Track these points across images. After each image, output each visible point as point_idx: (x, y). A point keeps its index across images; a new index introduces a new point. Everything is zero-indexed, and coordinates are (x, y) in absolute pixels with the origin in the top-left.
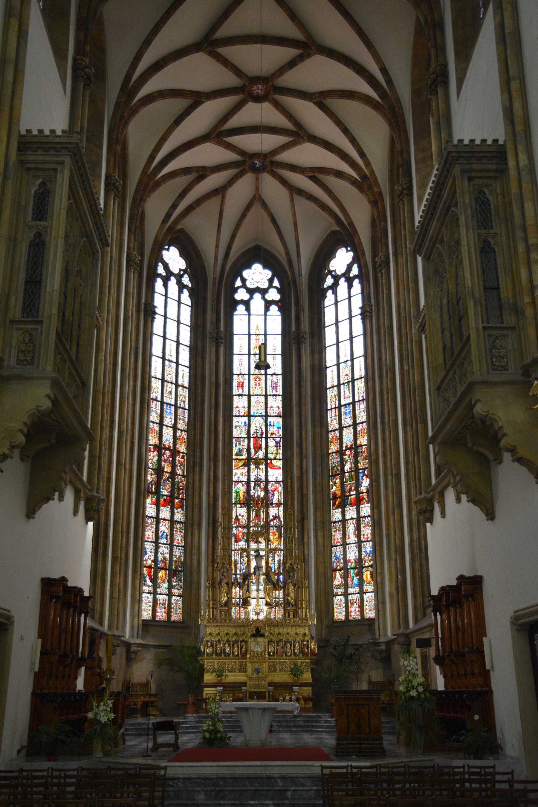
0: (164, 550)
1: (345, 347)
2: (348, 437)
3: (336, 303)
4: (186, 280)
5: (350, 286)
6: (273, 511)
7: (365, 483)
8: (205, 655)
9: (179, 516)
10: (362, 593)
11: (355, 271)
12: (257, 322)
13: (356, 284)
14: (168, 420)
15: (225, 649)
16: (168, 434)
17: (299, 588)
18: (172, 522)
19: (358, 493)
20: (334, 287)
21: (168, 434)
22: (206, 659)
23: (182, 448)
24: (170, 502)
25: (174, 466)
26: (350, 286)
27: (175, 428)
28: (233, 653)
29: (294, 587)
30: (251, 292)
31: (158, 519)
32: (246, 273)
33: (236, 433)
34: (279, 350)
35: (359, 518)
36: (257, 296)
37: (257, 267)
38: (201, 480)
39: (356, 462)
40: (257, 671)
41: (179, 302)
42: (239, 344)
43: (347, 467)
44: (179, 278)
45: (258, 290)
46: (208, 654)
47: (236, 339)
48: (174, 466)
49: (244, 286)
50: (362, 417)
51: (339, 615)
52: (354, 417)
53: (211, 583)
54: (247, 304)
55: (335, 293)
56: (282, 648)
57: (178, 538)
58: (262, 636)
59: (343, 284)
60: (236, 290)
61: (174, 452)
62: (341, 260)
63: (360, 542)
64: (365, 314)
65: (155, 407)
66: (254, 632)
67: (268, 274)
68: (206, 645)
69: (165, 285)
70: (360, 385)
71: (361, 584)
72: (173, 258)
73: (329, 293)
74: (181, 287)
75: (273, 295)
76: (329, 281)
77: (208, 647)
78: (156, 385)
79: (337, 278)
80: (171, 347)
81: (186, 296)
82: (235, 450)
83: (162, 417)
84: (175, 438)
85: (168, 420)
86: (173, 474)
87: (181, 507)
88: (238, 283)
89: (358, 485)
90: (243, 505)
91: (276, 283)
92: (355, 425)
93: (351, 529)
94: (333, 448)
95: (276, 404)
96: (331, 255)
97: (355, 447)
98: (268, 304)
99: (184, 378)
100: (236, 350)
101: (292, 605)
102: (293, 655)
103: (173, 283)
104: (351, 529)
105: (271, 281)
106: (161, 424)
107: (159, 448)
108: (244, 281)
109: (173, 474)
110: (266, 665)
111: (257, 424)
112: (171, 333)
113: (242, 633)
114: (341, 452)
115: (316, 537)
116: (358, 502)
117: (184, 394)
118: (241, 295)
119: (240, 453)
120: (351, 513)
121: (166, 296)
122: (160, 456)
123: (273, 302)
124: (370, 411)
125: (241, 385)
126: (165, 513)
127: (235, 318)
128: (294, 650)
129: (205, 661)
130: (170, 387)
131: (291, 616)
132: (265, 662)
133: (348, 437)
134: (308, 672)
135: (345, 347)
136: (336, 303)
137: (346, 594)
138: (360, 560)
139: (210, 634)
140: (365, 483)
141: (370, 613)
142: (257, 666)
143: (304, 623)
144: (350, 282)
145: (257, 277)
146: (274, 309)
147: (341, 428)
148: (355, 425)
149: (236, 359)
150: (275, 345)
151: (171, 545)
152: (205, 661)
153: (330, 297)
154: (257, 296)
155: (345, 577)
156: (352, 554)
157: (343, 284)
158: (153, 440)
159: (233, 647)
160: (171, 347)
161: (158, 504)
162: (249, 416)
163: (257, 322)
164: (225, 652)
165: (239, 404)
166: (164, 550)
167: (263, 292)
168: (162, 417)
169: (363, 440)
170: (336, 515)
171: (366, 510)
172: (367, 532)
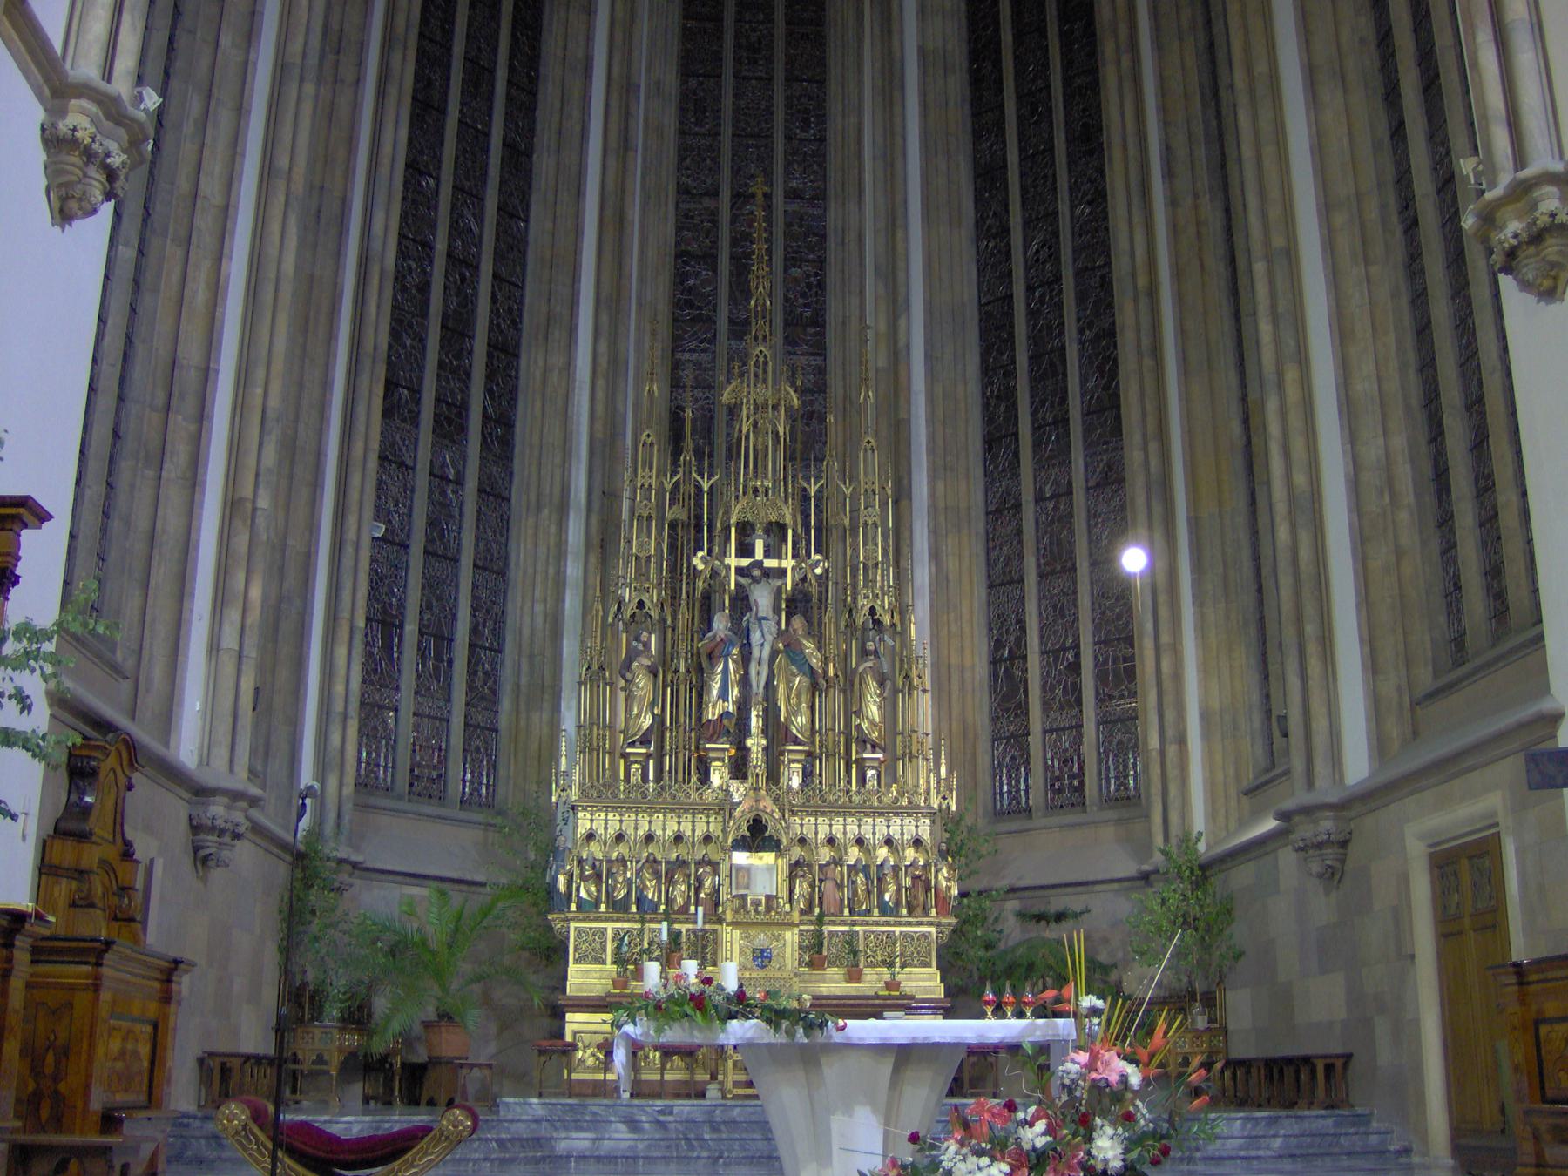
8: (573, 907)
15: (642, 889)
17: (895, 691)
22: (574, 919)
28: (669, 902)
29: (881, 684)
38: (569, 367)
40: (762, 957)
46: (581, 904)
53: (595, 667)
56: (840, 886)
58: (774, 845)
66: (744, 831)
68: (576, 871)
77: (583, 878)
101: (873, 747)
102: (876, 912)
110: (791, 937)
113: (699, 833)
115: (936, 556)
128: (881, 895)
129: (573, 925)
131: (872, 784)
132: (791, 925)
134: (926, 965)
139: (590, 836)
142: (761, 939)
152: (573, 925)
159: (670, 880)
164: (640, 901)
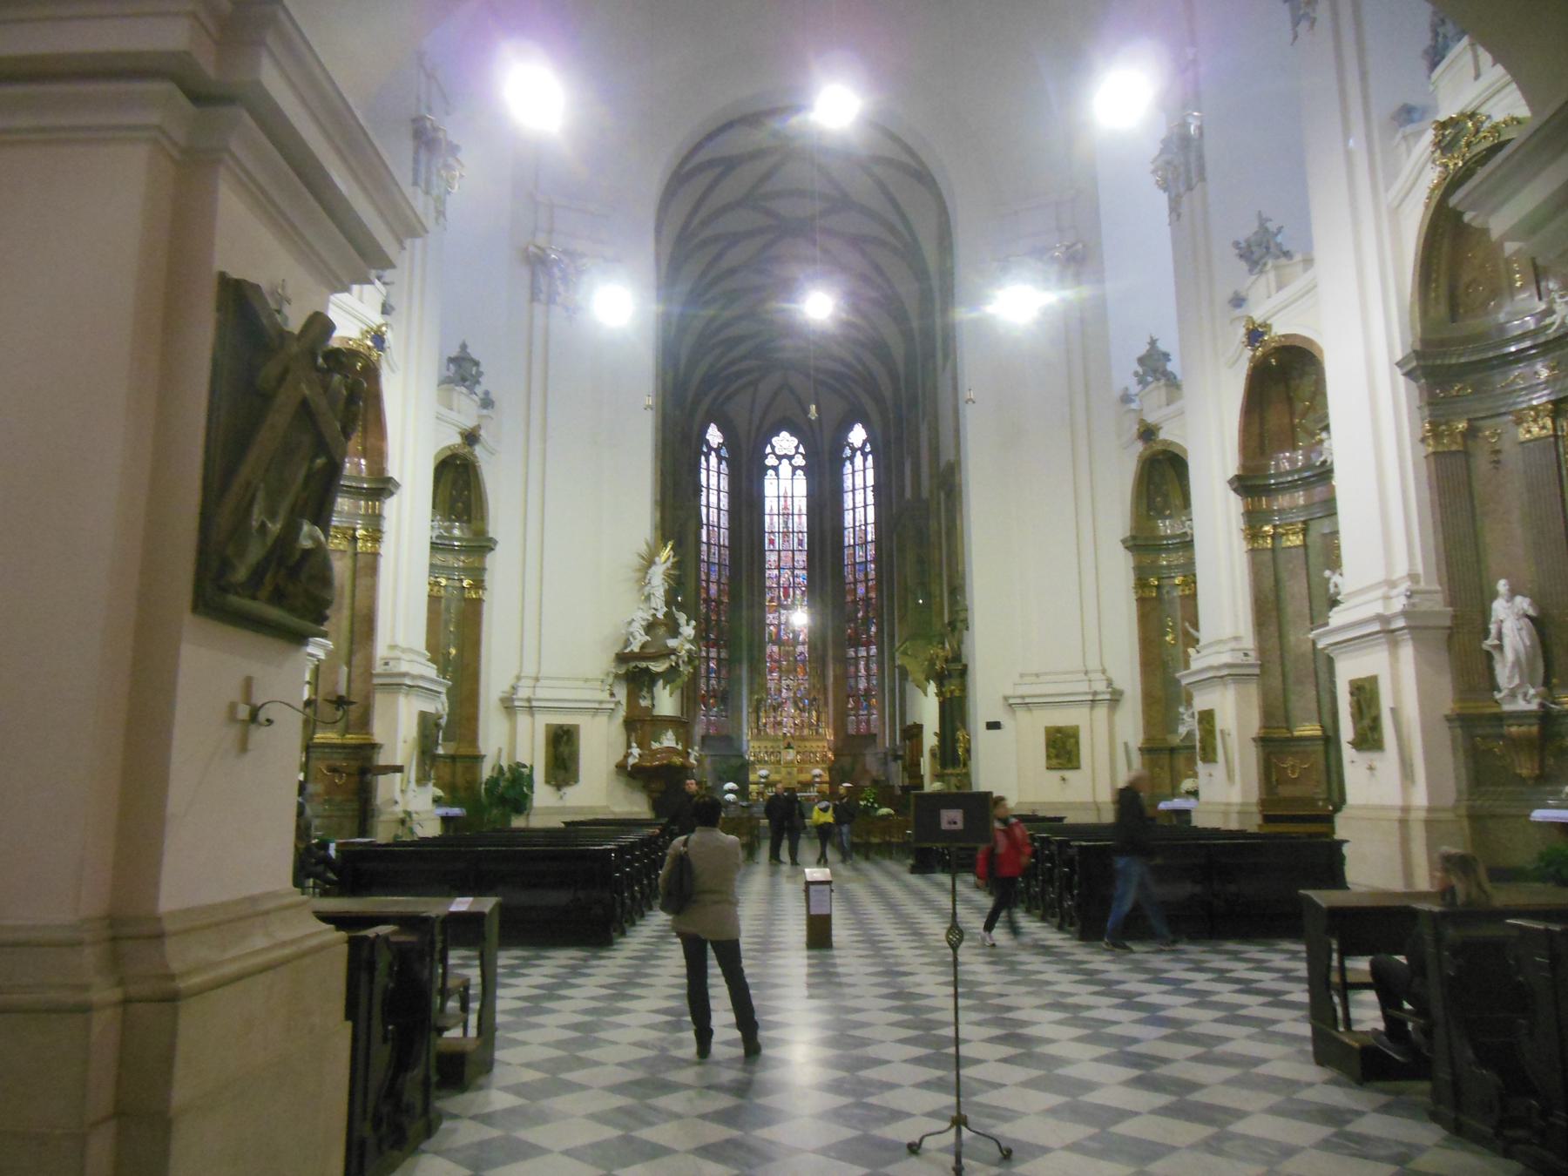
0: (713, 682)
1: (860, 512)
2: (861, 590)
3: (853, 472)
4: (724, 452)
5: (865, 460)
6: (800, 649)
7: (873, 629)
9: (723, 655)
10: (870, 714)
11: (868, 448)
12: (785, 484)
13: (870, 458)
14: (714, 577)
16: (713, 588)
18: (719, 660)
19: (869, 636)
20: (852, 459)
21: (713, 588)
23: (725, 600)
24: (716, 644)
25: (719, 615)
26: (865, 460)
27: (719, 582)
30: (780, 458)
31: (708, 659)
32: (775, 440)
33: (768, 583)
34: (804, 511)
35: (868, 658)
36: (785, 462)
37: (784, 435)
39: (866, 612)
41: (719, 473)
42: (770, 504)
43: (860, 615)
44: (717, 451)
45: (785, 456)
47: (767, 501)
48: (719, 615)
49: (773, 452)
50: (872, 575)
51: (852, 730)
52: (866, 575)
54: (775, 469)
55: (852, 463)
57: (724, 672)
59: (859, 458)
60: (766, 456)
61: (719, 603)
62: (858, 435)
63: (868, 677)
64: (876, 489)
65: (704, 567)
67: (795, 441)
69: (707, 461)
70: (871, 547)
71: (869, 707)
72: (714, 436)
73: (848, 464)
74: (720, 459)
75: (799, 461)
76: (848, 452)
78: (704, 547)
79: (854, 450)
80: (713, 512)
81: (724, 466)
82: (768, 597)
83: (708, 575)
84: (719, 590)
85: (714, 577)
86: (718, 621)
87: (725, 646)
88: (768, 450)
89: (868, 630)
90: (774, 643)
91: (801, 450)
92: (867, 580)
93: (862, 664)
94: (849, 598)
95: (801, 558)
96: (850, 428)
97: (867, 600)
98: (795, 469)
99: (724, 541)
100: (767, 511)
103: (713, 459)
104: (862, 664)
105: (797, 448)
106: (708, 581)
107: (708, 601)
108: (773, 447)
109: (718, 621)
111: (786, 574)
112: (714, 499)
114: (855, 602)
116: (867, 644)
117: (725, 552)
118: (771, 461)
119: (771, 600)
120: (862, 652)
121: (708, 470)
122: (708, 607)
123: (799, 467)
124: (878, 570)
125: (772, 542)
126: (713, 653)
127: (767, 483)
130: (714, 549)
133: (861, 590)
135: (860, 512)
136: (853, 472)
137: (857, 715)
138: (868, 690)
140: (873, 629)
141: (874, 730)
143: (824, 738)
144: (865, 455)
145: (785, 444)
146: (799, 472)
147: (855, 582)
148: (867, 580)
149: (767, 518)
150: (801, 504)
151: (718, 678)
153: (848, 467)
154: (785, 462)
155: (857, 702)
156: (862, 685)
157: (859, 458)
158: (704, 595)
160: (713, 512)
161: (707, 647)
162: (779, 568)
163: (785, 484)
165: (771, 558)
166: (713, 682)
167: (790, 458)
168: (708, 575)
169: (873, 595)
170: (851, 653)
171: (873, 650)
172: (874, 667)
